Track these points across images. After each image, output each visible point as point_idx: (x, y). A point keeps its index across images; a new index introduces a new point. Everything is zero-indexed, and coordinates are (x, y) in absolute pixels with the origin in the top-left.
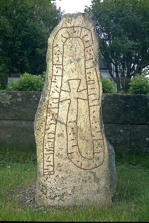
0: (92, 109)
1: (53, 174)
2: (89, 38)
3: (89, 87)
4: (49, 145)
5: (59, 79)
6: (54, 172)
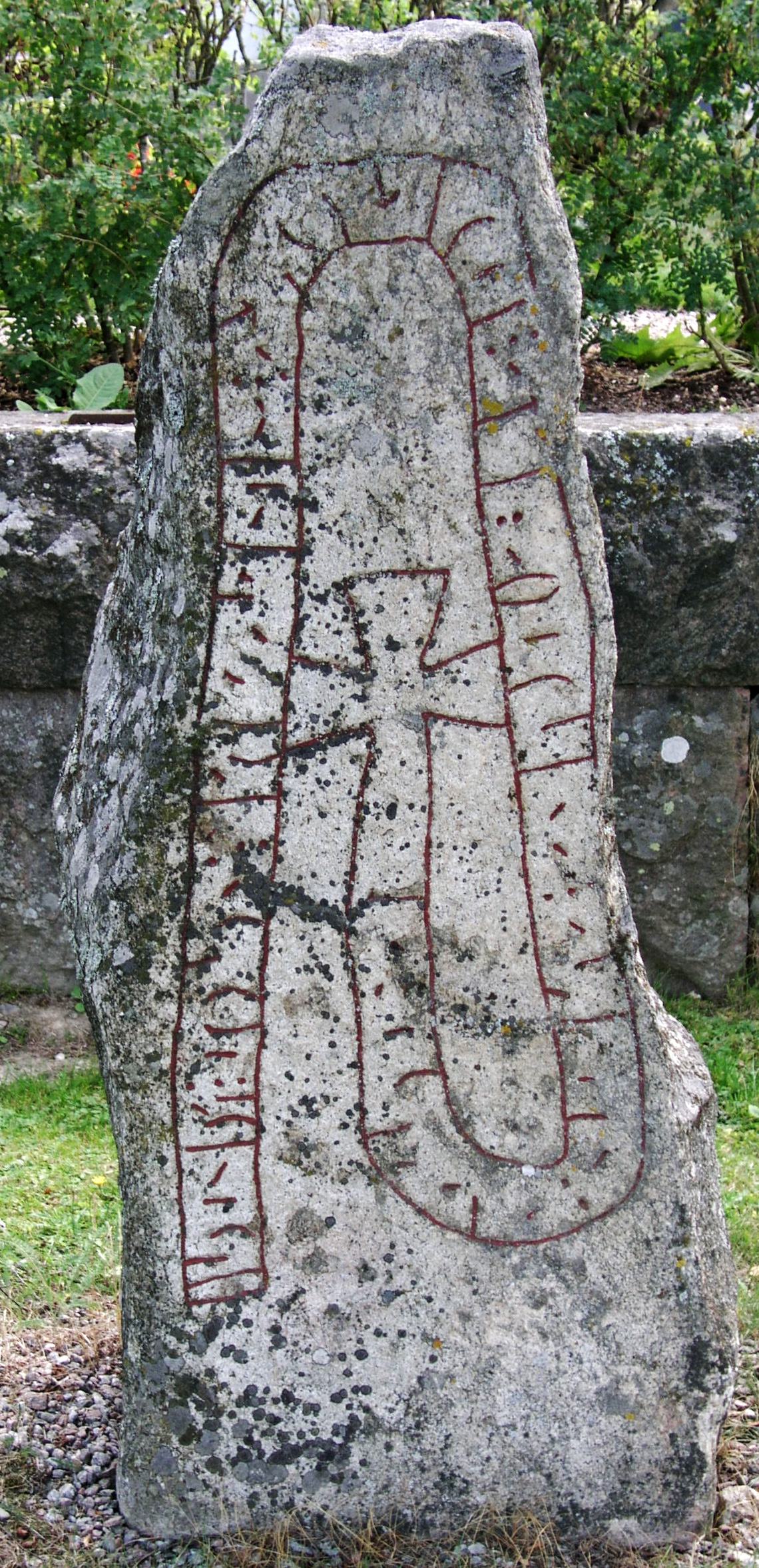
0: (545, 790)
1: (258, 1294)
2: (504, 242)
3: (510, 625)
4: (219, 1083)
5: (273, 581)
6: (266, 1278)
